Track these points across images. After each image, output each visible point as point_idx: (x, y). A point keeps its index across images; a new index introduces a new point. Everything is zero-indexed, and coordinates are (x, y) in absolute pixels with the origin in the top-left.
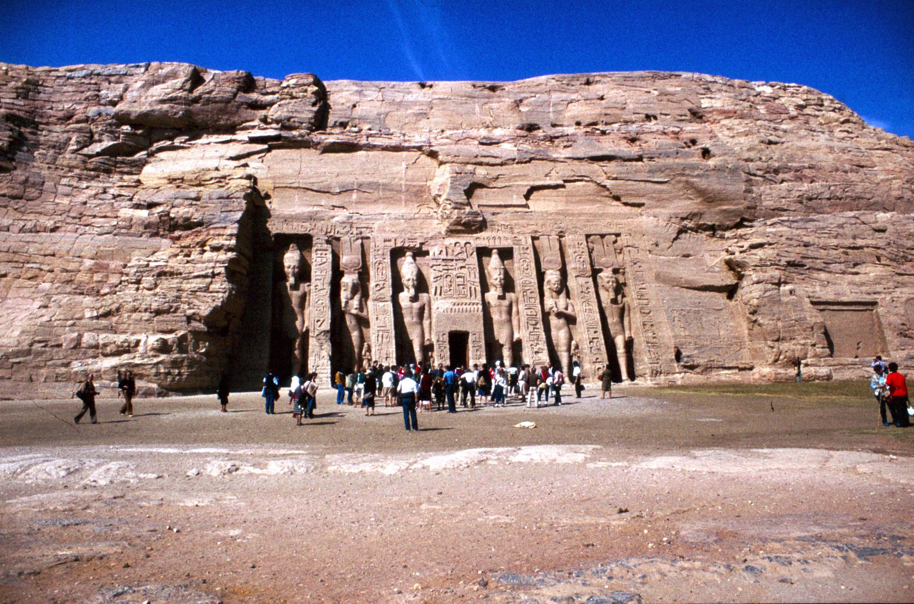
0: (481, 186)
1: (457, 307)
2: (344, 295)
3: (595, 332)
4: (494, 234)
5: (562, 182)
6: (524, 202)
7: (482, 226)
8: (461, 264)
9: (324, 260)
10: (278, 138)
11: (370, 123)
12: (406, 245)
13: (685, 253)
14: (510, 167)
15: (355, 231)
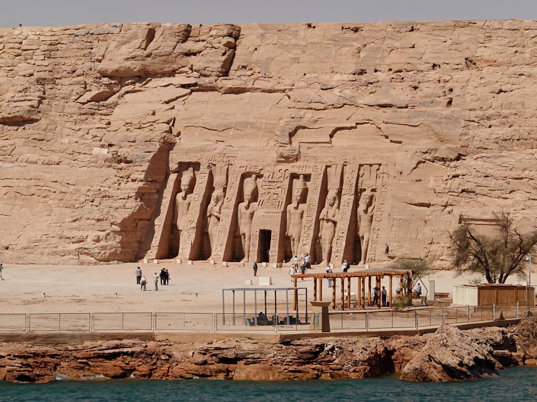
0: (304, 128)
1: (267, 214)
2: (212, 202)
3: (343, 233)
4: (305, 164)
5: (354, 125)
6: (328, 139)
7: (297, 159)
8: (278, 185)
9: (203, 180)
10: (196, 84)
11: (260, 67)
12: (251, 171)
13: (418, 179)
14: (330, 111)
15: (225, 159)
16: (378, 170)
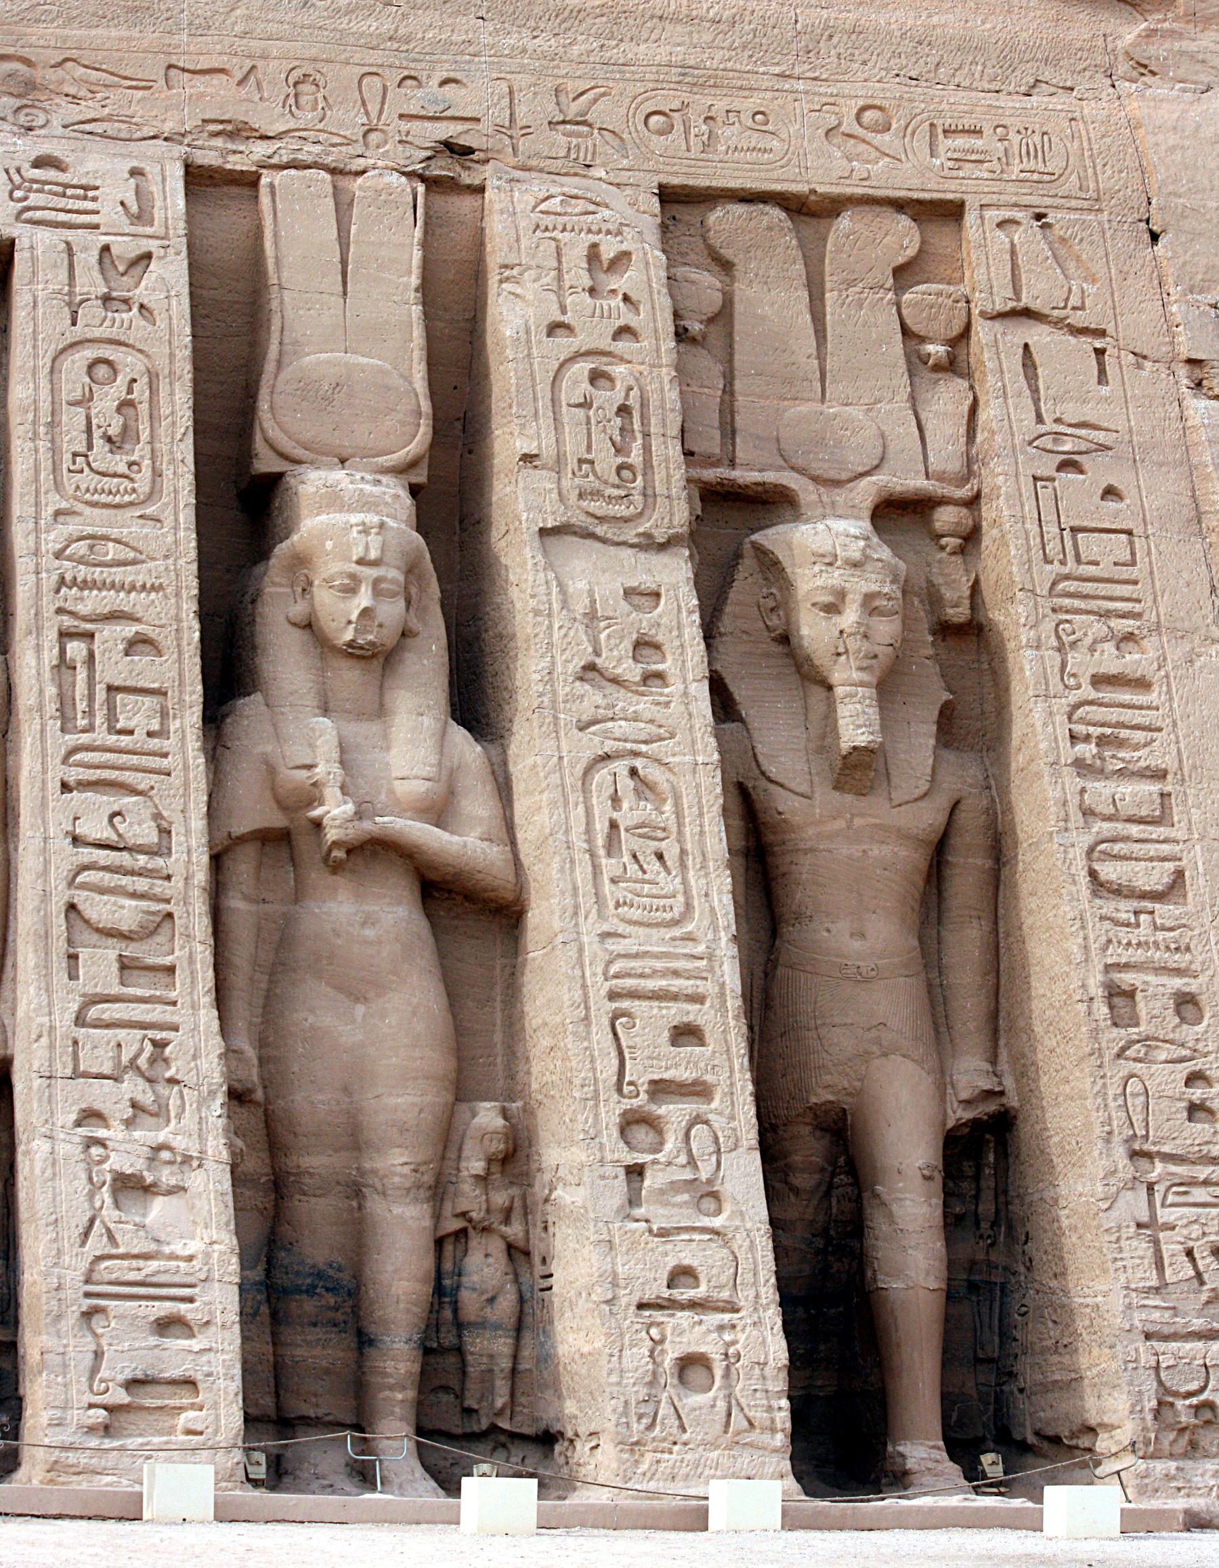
3: (686, 1034)
16: (904, 274)
